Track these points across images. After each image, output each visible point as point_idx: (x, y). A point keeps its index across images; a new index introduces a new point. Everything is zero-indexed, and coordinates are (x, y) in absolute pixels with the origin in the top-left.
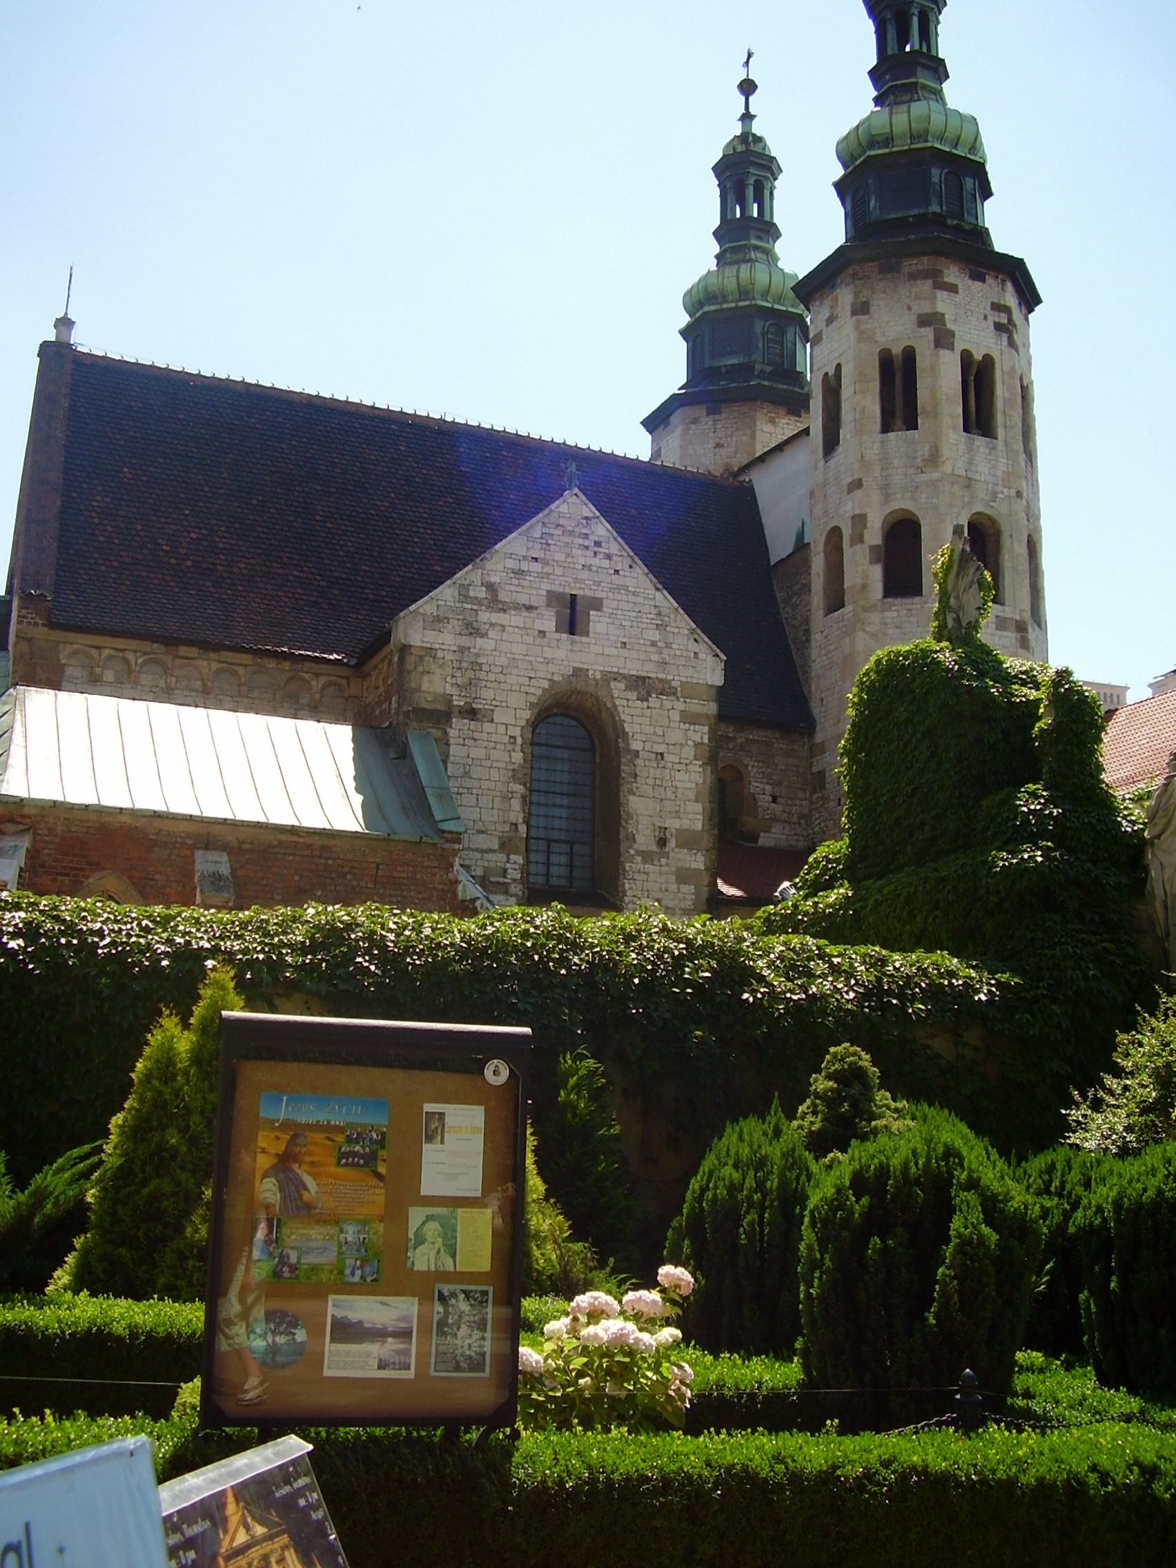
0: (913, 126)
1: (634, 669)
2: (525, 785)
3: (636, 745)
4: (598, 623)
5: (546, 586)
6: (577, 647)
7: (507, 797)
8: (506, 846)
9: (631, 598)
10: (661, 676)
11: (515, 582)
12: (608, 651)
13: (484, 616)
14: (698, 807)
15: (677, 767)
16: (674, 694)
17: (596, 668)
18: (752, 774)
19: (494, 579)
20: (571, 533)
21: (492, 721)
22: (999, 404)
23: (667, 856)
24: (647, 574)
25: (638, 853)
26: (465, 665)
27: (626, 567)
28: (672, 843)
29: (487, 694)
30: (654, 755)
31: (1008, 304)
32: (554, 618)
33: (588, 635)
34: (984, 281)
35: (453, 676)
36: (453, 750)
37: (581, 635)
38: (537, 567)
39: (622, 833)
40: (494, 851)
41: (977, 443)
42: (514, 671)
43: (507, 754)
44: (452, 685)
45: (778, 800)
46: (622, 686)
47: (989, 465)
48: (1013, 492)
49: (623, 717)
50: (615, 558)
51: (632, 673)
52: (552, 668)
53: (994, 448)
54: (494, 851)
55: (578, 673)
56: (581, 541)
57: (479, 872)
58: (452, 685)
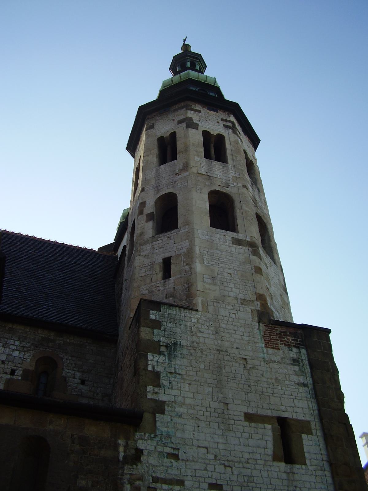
0: (182, 77)
18: (65, 364)
34: (217, 112)
45: (86, 382)
47: (222, 172)
48: (240, 185)
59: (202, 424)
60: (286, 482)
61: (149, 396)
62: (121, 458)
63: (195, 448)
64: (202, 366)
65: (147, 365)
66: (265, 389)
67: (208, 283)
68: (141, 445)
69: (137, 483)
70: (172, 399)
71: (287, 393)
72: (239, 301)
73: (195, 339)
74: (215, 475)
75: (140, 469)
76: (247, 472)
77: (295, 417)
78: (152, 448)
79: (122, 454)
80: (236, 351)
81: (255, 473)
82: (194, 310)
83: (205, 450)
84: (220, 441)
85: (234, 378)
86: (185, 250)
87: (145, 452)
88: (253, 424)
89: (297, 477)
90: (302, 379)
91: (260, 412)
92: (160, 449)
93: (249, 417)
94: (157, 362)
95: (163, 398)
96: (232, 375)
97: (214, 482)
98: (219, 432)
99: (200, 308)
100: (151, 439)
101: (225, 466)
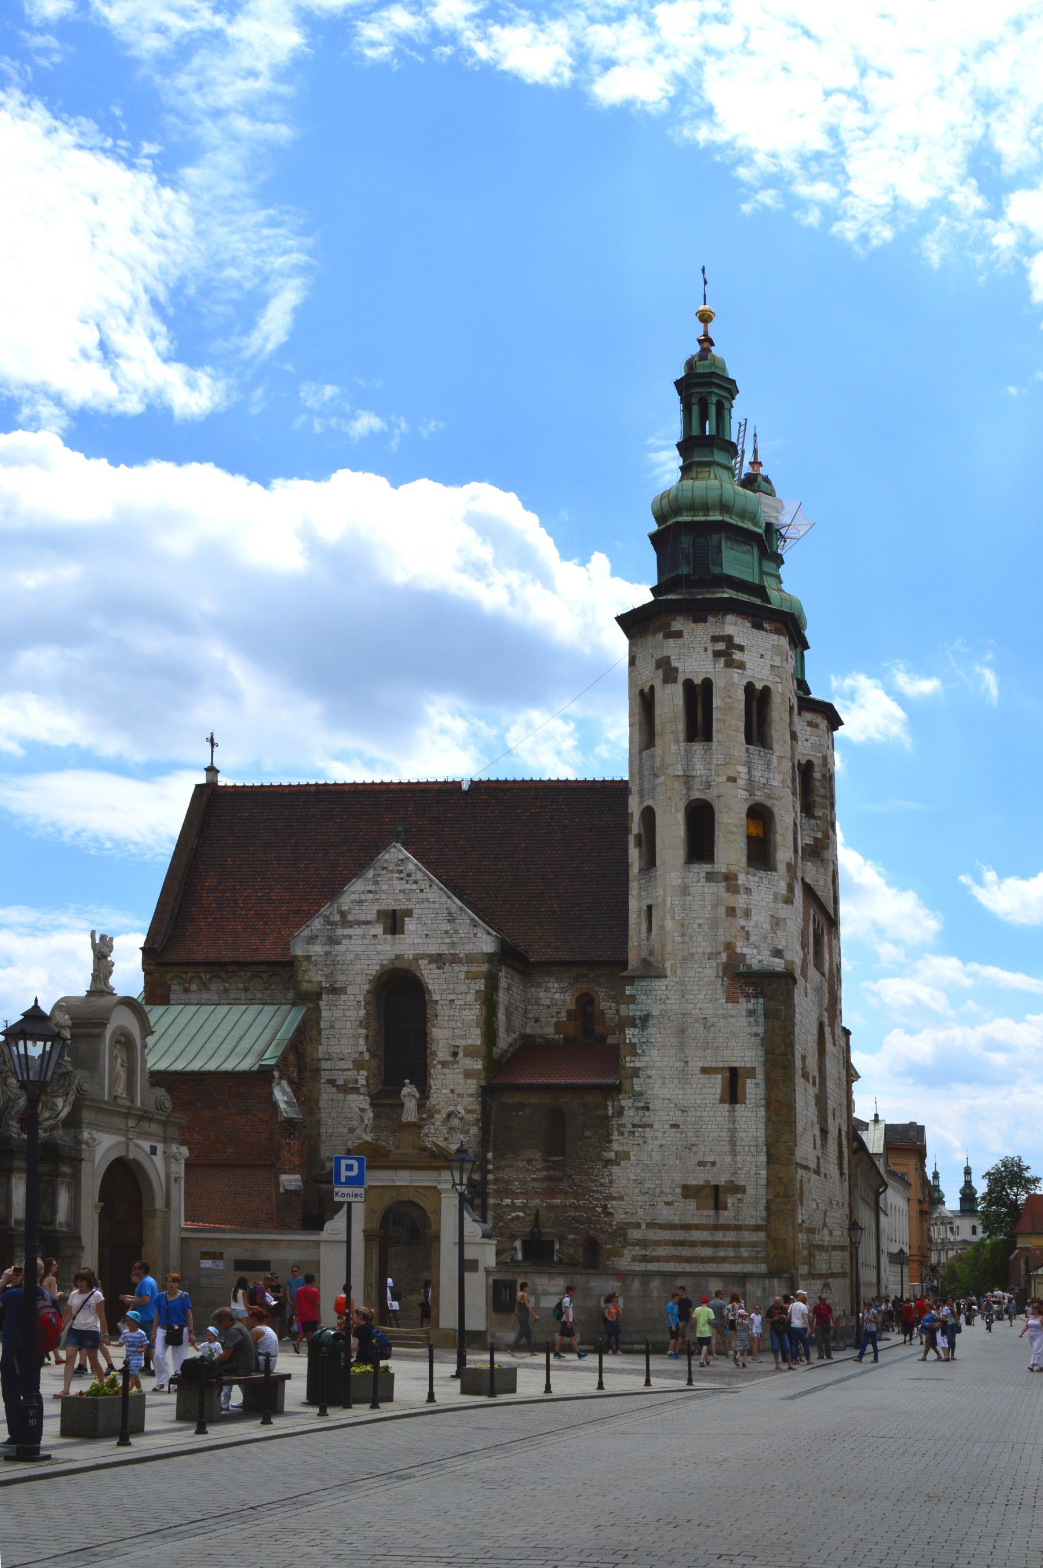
2: (366, 1028)
3: (436, 997)
4: (410, 925)
5: (378, 908)
6: (398, 940)
7: (356, 1037)
8: (358, 1065)
9: (431, 906)
11: (357, 907)
12: (416, 941)
13: (340, 932)
14: (478, 1031)
15: (465, 1007)
16: (461, 962)
17: (409, 953)
21: (346, 994)
22: (715, 714)
23: (457, 1062)
24: (441, 889)
25: (439, 1062)
26: (328, 962)
27: (428, 887)
28: (461, 1054)
29: (341, 978)
30: (447, 1002)
32: (382, 926)
33: (403, 933)
35: (322, 970)
37: (399, 934)
39: (429, 1051)
40: (349, 1070)
41: (694, 748)
42: (358, 962)
43: (355, 1013)
44: (322, 975)
47: (703, 763)
48: (723, 779)
49: (427, 980)
51: (433, 952)
52: (381, 957)
53: (710, 749)
54: (349, 1070)
58: (322, 975)
59: (667, 1081)
60: (727, 1119)
61: (628, 1065)
62: (610, 1114)
63: (661, 1101)
64: (669, 1032)
65: (626, 1039)
66: (720, 1044)
67: (680, 943)
68: (623, 1103)
70: (645, 1064)
71: (739, 1044)
72: (706, 956)
73: (664, 1007)
74: (675, 1118)
75: (623, 1121)
76: (698, 1114)
77: (743, 1065)
79: (610, 1112)
80: (697, 1012)
81: (705, 1114)
82: (662, 977)
83: (668, 1101)
84: (680, 1092)
85: (695, 1038)
86: (660, 900)
87: (626, 1108)
88: (707, 1076)
89: (737, 1114)
90: (754, 1030)
91: (714, 1065)
92: (637, 1104)
93: (705, 1070)
94: (633, 1035)
95: (638, 1064)
96: (693, 1036)
97: (673, 1123)
98: (679, 1086)
99: (669, 973)
100: (630, 1098)
101: (683, 1111)
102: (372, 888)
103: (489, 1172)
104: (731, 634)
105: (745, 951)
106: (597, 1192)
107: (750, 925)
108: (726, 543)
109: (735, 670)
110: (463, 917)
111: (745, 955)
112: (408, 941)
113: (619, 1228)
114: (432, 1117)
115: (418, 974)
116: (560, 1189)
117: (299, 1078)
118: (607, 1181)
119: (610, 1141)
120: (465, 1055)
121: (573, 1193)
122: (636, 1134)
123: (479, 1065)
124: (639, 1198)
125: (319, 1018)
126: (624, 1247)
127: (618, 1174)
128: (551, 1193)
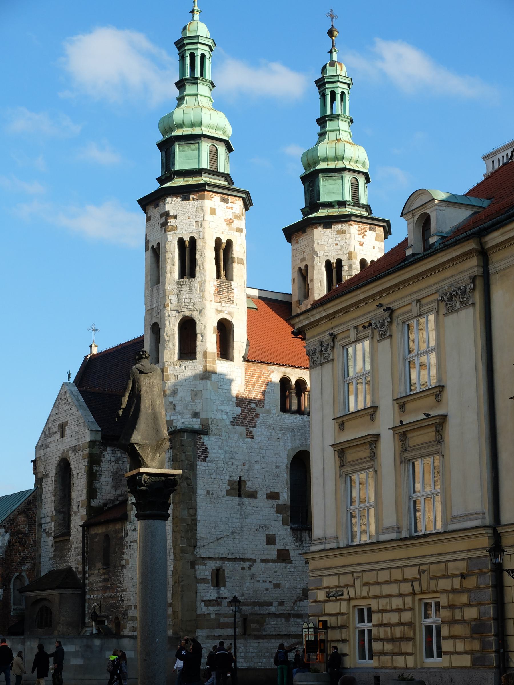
1: (73, 444)
4: (67, 432)
5: (58, 423)
10: (78, 444)
14: (85, 491)
19: (50, 426)
20: (63, 400)
28: (80, 507)
30: (77, 475)
31: (165, 211)
36: (44, 490)
38: (57, 416)
46: (70, 452)
49: (71, 463)
50: (70, 404)
55: (64, 450)
56: (64, 402)
57: (47, 531)
62: (123, 536)
69: (127, 545)
75: (128, 539)
78: (130, 528)
102: (57, 412)
103: (87, 579)
104: (167, 210)
105: (172, 418)
106: (119, 587)
107: (176, 400)
108: (179, 148)
109: (169, 233)
110: (82, 422)
111: (173, 420)
112: (66, 441)
113: (125, 610)
114: (71, 547)
115: (69, 460)
116: (108, 587)
117: (28, 530)
118: (122, 579)
119: (123, 554)
120: (81, 507)
121: (112, 588)
122: (132, 547)
123: (83, 512)
124: (132, 589)
125: (41, 493)
126: (127, 622)
127: (126, 575)
128: (105, 589)
